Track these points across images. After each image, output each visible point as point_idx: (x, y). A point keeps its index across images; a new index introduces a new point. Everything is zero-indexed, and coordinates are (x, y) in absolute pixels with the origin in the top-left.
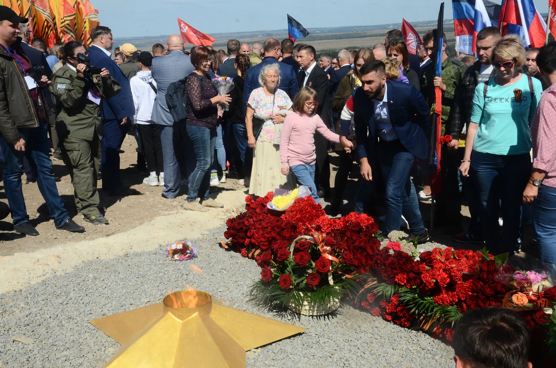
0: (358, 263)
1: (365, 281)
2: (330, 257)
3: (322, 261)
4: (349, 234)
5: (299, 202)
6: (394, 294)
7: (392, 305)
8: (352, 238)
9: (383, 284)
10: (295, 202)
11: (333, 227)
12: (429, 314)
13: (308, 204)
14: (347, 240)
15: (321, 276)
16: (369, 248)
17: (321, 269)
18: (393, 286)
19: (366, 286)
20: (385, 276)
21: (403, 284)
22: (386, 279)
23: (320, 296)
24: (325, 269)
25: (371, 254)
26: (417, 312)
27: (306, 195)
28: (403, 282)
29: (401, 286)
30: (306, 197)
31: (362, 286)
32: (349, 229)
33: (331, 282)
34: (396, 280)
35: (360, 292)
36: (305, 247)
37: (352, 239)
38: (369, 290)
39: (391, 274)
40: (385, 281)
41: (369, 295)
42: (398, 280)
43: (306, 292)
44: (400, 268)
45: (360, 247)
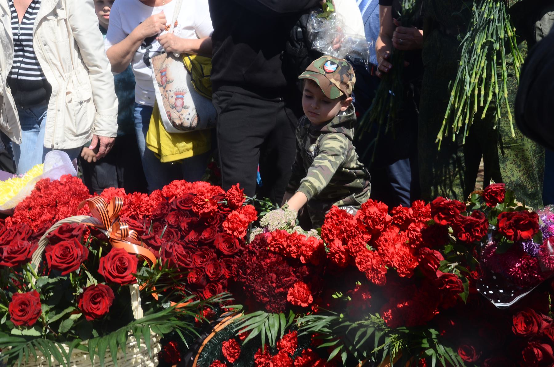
0: (197, 279)
1: (215, 319)
2: (136, 249)
3: (117, 257)
4: (171, 220)
5: (47, 187)
6: (286, 332)
7: (282, 356)
8: (179, 227)
9: (260, 312)
10: (38, 189)
11: (135, 210)
12: (376, 349)
13: (70, 189)
14: (169, 233)
15: (115, 290)
16: (221, 239)
17: (115, 273)
18: (283, 316)
19: (218, 328)
20: (263, 293)
21: (304, 305)
22: (266, 299)
23: (113, 342)
24: (124, 274)
25: (226, 253)
26: (344, 356)
27: (64, 173)
28: (306, 301)
29: (303, 312)
30: (63, 177)
31: (208, 329)
32: (173, 210)
33: (138, 313)
34: (290, 298)
35: (205, 342)
36: (74, 233)
37: (181, 230)
38: (228, 333)
39: (278, 287)
40: (262, 307)
41: (226, 344)
42: (294, 297)
43: (75, 342)
44: (295, 272)
45: (201, 243)
